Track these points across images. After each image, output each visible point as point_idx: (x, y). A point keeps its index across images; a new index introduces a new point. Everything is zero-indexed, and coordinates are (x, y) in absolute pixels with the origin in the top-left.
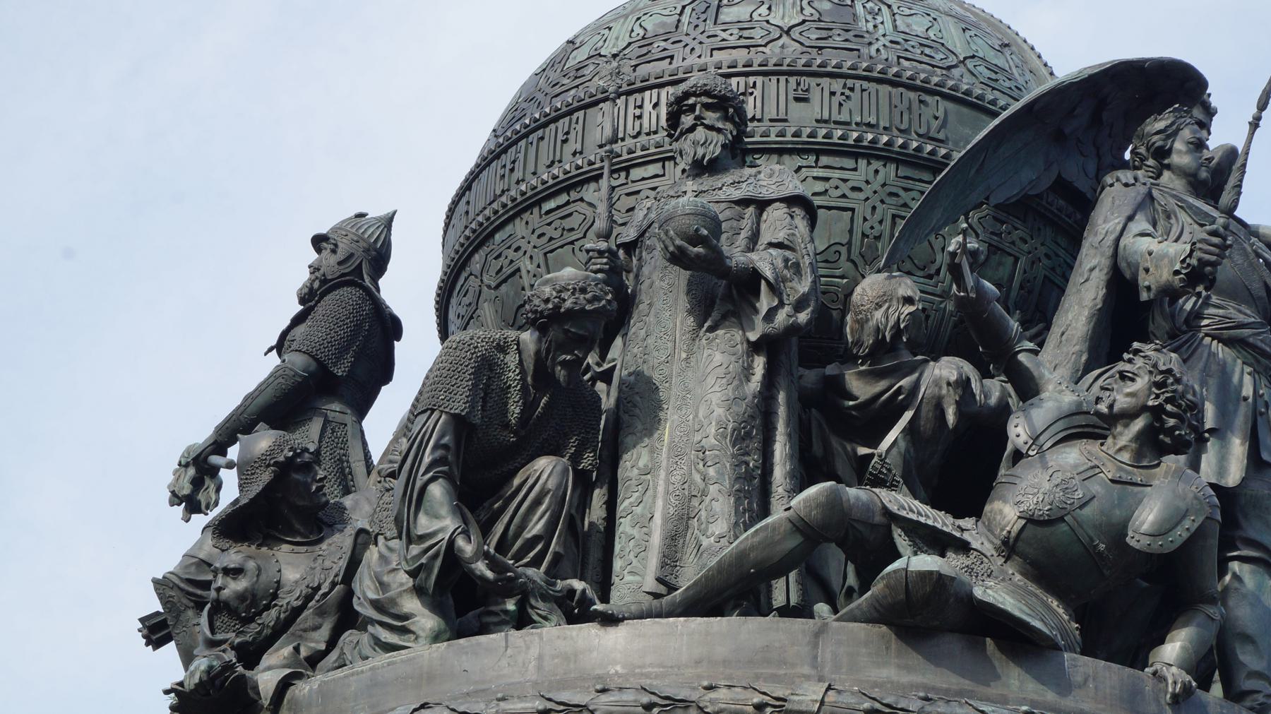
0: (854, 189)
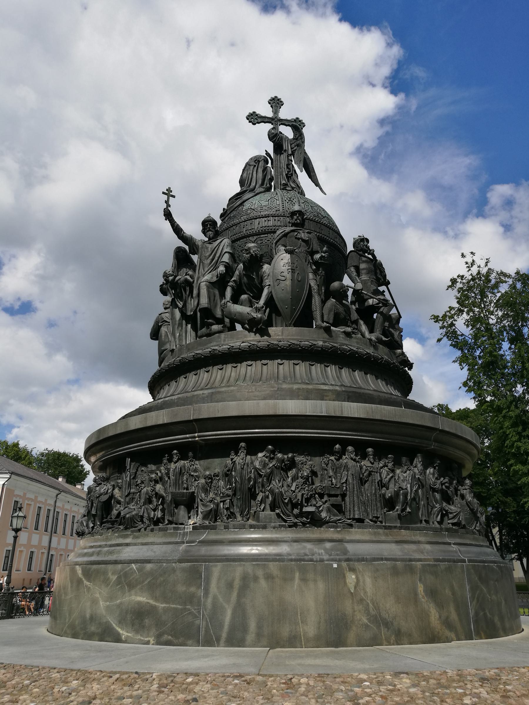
0: (268, 241)
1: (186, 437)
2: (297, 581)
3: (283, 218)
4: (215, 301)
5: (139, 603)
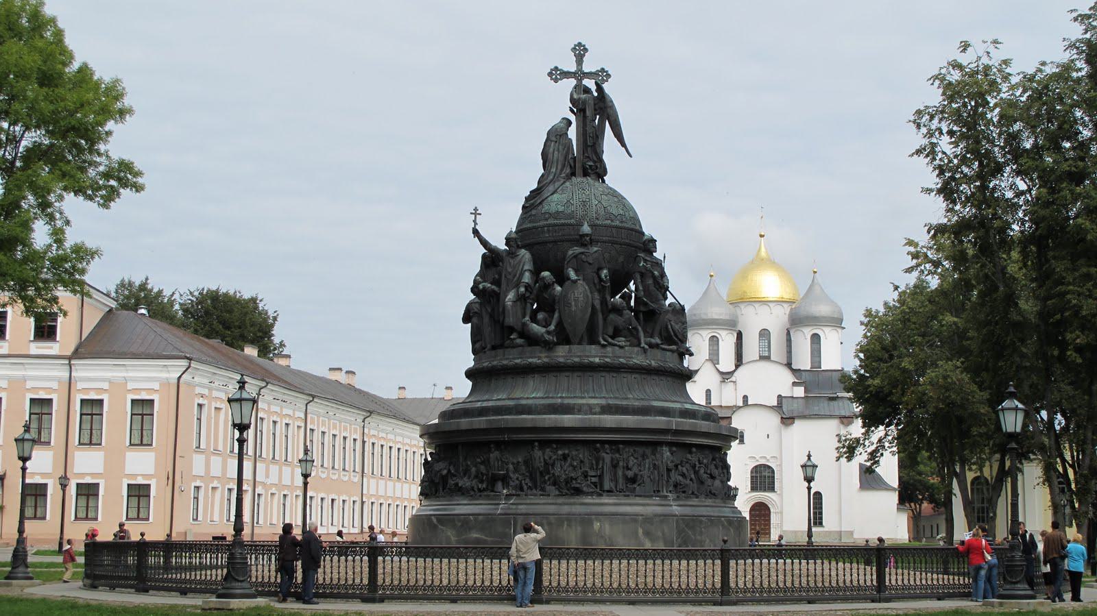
1: (500, 437)
2: (565, 526)
5: (476, 538)
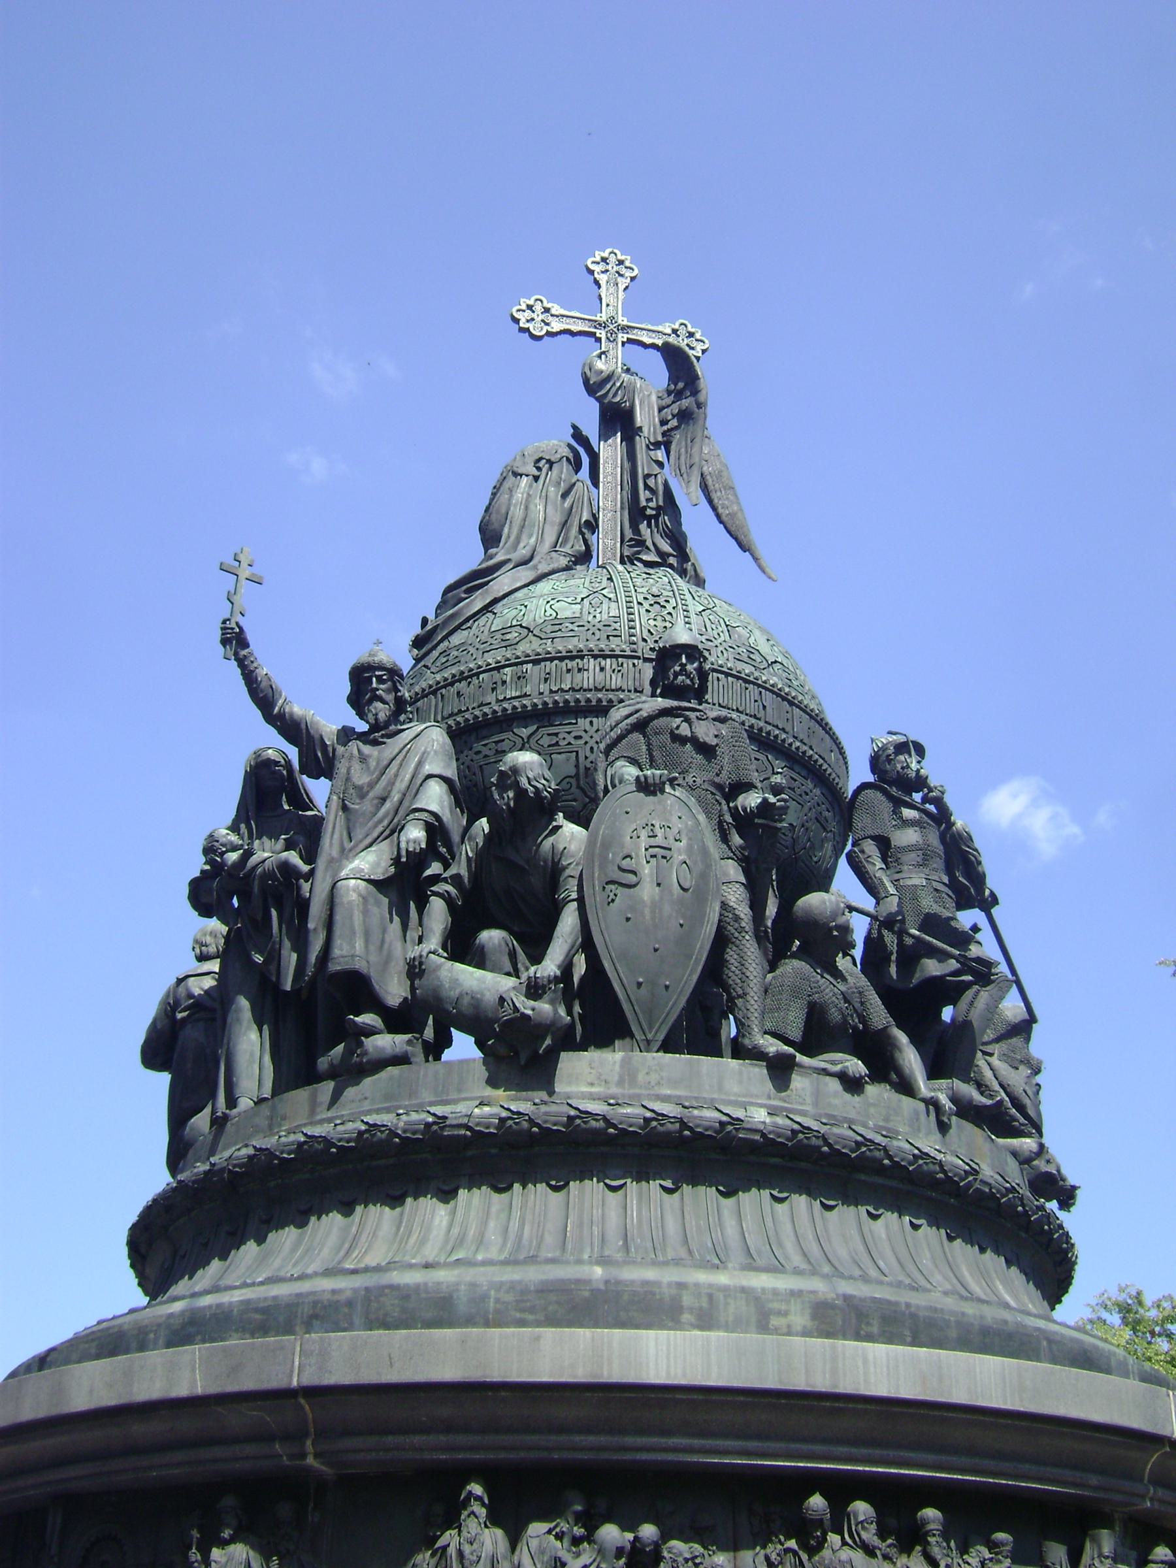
0: (576, 738)
3: (630, 662)
4: (386, 946)
